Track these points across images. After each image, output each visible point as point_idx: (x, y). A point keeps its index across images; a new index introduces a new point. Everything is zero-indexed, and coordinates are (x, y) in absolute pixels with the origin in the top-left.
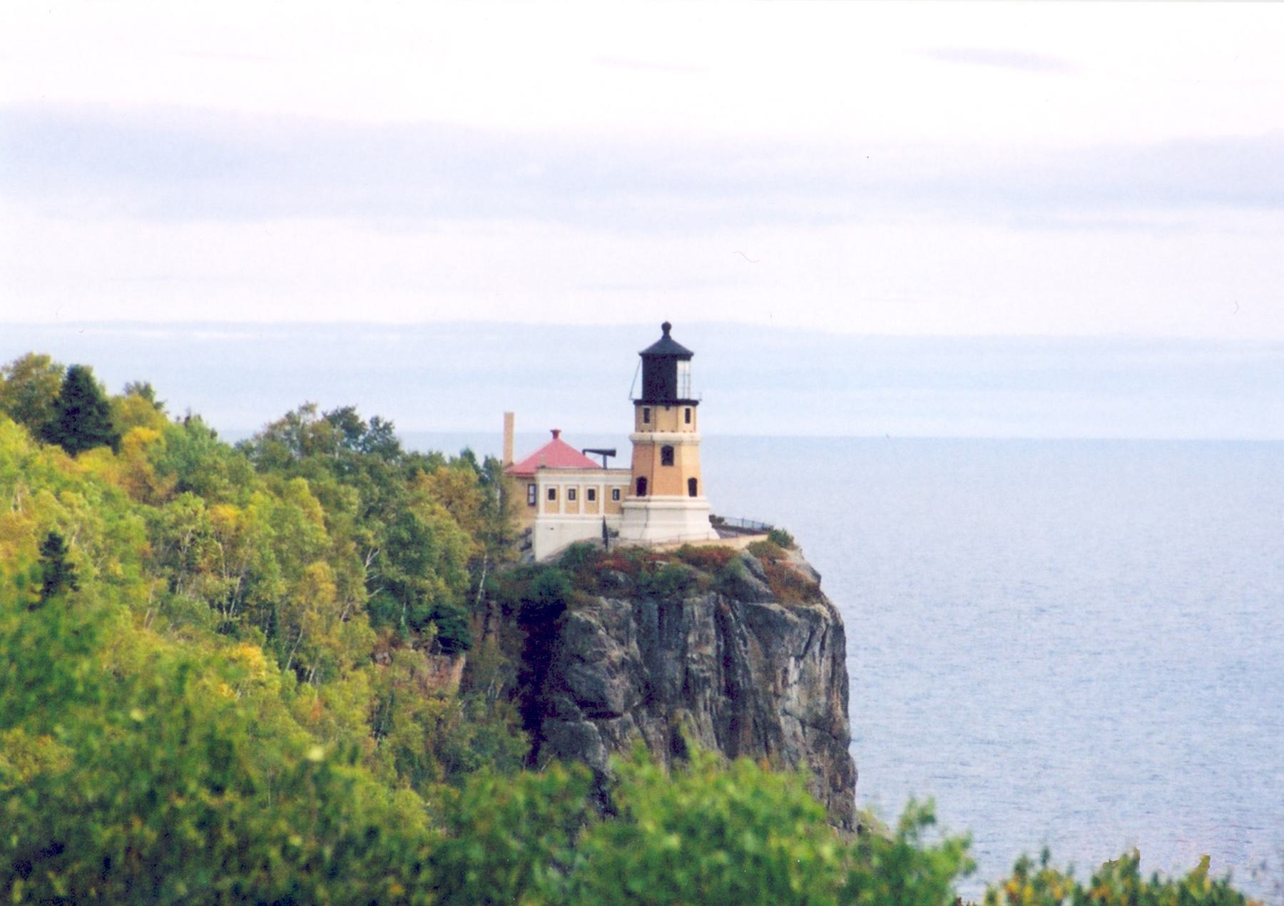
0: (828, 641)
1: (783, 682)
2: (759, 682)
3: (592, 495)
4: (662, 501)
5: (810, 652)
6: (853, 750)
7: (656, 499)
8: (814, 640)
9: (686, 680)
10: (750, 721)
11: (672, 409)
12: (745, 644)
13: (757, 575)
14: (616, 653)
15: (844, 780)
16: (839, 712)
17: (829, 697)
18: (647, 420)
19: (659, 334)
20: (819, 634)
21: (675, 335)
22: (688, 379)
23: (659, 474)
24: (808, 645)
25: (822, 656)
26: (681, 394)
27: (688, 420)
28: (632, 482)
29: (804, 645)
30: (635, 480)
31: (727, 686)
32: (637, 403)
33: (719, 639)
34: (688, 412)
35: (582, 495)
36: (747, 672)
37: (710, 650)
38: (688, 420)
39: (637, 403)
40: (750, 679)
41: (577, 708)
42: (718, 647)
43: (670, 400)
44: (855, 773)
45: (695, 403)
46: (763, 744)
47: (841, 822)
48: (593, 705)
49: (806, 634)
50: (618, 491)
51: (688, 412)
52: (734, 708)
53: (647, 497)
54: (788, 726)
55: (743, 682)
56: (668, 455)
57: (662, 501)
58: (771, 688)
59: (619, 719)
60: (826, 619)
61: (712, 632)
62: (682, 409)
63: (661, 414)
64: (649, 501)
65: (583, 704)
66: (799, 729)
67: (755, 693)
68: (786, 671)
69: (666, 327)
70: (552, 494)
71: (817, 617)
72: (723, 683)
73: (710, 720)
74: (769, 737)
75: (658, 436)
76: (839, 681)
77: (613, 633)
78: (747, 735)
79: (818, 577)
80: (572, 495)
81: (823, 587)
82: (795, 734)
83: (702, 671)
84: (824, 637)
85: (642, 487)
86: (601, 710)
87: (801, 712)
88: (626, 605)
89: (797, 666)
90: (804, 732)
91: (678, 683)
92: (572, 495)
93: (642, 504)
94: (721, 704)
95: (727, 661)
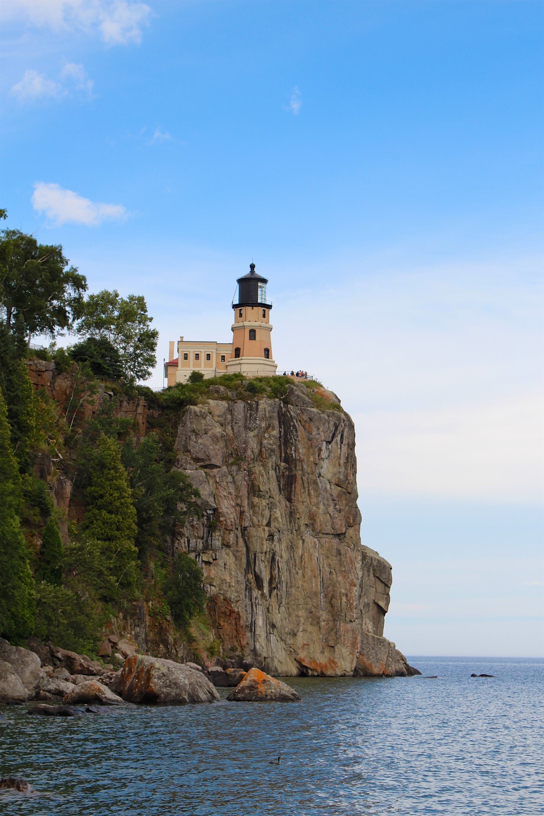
0: (345, 434)
1: (319, 456)
2: (304, 455)
3: (208, 357)
4: (248, 359)
5: (335, 440)
6: (359, 502)
7: (244, 359)
8: (338, 432)
9: (261, 449)
10: (300, 477)
11: (255, 308)
12: (296, 431)
13: (304, 394)
14: (218, 430)
15: (354, 521)
16: (351, 477)
17: (346, 468)
18: (241, 315)
20: (340, 429)
23: (248, 345)
24: (334, 436)
25: (342, 443)
26: (259, 301)
27: (264, 316)
28: (232, 351)
29: (331, 435)
30: (234, 350)
31: (285, 456)
32: (235, 306)
33: (280, 427)
34: (264, 310)
35: (203, 357)
37: (275, 433)
38: (264, 316)
39: (235, 306)
40: (299, 453)
41: (192, 462)
42: (280, 432)
43: (255, 304)
44: (361, 517)
45: (269, 307)
46: (307, 492)
47: (353, 545)
48: (203, 460)
49: (332, 428)
50: (223, 358)
51: (264, 310)
52: (289, 469)
53: (240, 358)
54: (323, 483)
55: (295, 455)
56: (253, 334)
57: (248, 359)
58: (312, 459)
59: (219, 469)
60: (344, 420)
61: (276, 423)
62: (261, 309)
63: (248, 311)
64: (242, 360)
65: (197, 460)
66: (328, 487)
67: (301, 461)
68: (320, 450)
69: (252, 267)
71: (339, 419)
72: (283, 455)
73: (275, 476)
74: (310, 489)
75: (246, 323)
77: (216, 418)
79: (340, 401)
80: (197, 356)
81: (342, 404)
82: (326, 488)
83: (270, 444)
84: (343, 431)
85: (237, 353)
86: (207, 463)
87: (329, 476)
88: (224, 404)
89: (327, 449)
90: (331, 488)
91: (256, 451)
92: (197, 356)
93: (238, 362)
94: (282, 468)
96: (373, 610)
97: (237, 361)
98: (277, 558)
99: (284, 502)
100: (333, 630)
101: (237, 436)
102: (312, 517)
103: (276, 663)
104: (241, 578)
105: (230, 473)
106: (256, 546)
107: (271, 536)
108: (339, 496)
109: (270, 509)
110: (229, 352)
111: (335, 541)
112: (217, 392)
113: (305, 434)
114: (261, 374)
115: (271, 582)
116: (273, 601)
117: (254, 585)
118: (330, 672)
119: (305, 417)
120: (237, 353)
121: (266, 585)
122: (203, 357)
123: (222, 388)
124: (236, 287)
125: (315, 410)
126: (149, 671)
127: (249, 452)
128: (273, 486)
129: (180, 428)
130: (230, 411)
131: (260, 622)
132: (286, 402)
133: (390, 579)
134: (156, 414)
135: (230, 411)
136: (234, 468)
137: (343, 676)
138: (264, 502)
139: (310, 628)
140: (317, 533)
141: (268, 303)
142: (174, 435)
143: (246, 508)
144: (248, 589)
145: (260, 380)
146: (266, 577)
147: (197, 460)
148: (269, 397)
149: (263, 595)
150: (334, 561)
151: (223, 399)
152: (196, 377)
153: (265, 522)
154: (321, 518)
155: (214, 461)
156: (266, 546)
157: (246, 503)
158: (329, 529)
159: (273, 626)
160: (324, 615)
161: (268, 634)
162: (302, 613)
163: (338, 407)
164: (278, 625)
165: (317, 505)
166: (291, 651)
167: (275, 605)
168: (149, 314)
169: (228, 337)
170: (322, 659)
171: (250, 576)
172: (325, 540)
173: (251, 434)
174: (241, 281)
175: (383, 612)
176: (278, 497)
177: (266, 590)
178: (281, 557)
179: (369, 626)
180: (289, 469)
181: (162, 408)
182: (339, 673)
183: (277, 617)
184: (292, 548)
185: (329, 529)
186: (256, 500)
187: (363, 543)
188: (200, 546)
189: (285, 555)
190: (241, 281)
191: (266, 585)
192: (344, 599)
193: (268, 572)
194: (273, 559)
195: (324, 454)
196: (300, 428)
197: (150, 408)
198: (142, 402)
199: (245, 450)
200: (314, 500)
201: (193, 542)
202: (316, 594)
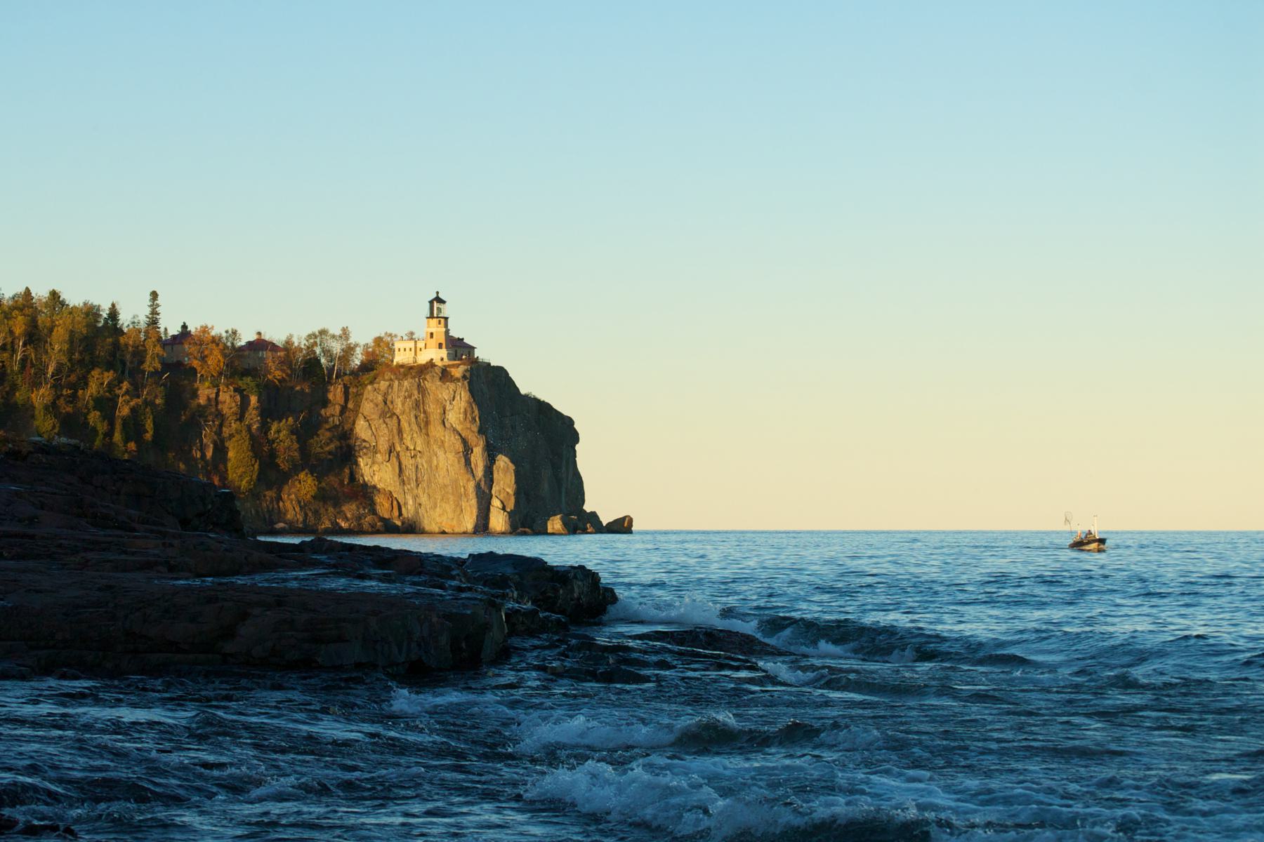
3: (411, 350)
19: (435, 296)
21: (440, 296)
35: (408, 350)
45: (446, 319)
61: (416, 392)
69: (438, 293)
78: (431, 428)
80: (405, 350)
88: (387, 383)
92: (405, 350)
98: (420, 467)
115: (416, 481)
118: (457, 530)
122: (408, 350)
124: (428, 304)
141: (445, 316)
144: (403, 483)
153: (412, 448)
157: (397, 437)
165: (444, 436)
177: (413, 484)
178: (423, 466)
180: (427, 418)
182: (462, 529)
184: (430, 462)
190: (431, 302)
192: (462, 489)
193: (414, 475)
194: (417, 467)
196: (431, 394)
202: (446, 486)
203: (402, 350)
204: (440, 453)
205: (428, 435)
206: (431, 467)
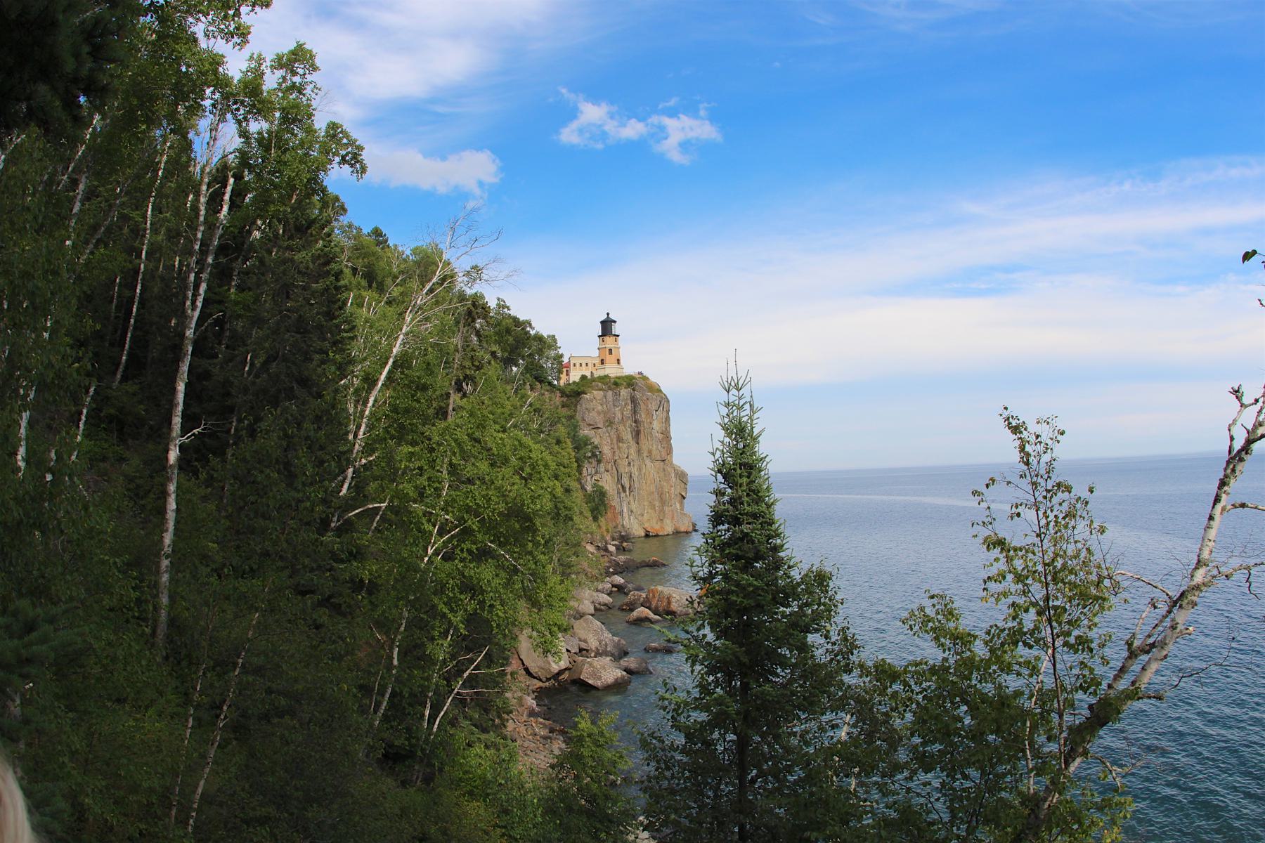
7: (607, 365)
22: (616, 329)
23: (608, 358)
32: (599, 336)
35: (584, 365)
36: (640, 416)
37: (629, 407)
45: (618, 336)
63: (607, 338)
67: (643, 422)
69: (608, 314)
70: (575, 365)
76: (668, 419)
78: (642, 436)
80: (581, 365)
85: (602, 362)
92: (581, 365)
95: (635, 412)
96: (679, 497)
97: (602, 366)
99: (635, 445)
100: (662, 511)
101: (609, 410)
102: (650, 452)
103: (634, 531)
104: (615, 487)
105: (607, 431)
106: (621, 470)
107: (629, 463)
108: (663, 439)
109: (628, 449)
110: (597, 361)
111: (662, 463)
112: (597, 386)
113: (645, 407)
114: (618, 375)
116: (631, 497)
117: (621, 490)
118: (660, 534)
119: (645, 398)
120: (602, 362)
121: (627, 490)
122: (584, 365)
123: (600, 384)
124: (599, 327)
125: (649, 394)
126: (668, 598)
127: (616, 419)
128: (630, 436)
129: (578, 407)
130: (605, 396)
131: (625, 510)
132: (634, 390)
133: (687, 480)
134: (565, 399)
135: (605, 396)
136: (609, 428)
137: (668, 535)
138: (625, 446)
139: (650, 511)
140: (652, 461)
142: (575, 411)
143: (616, 450)
144: (619, 493)
145: (619, 378)
146: (627, 486)
147: (590, 425)
148: (625, 388)
149: (626, 496)
150: (662, 474)
151: (600, 390)
152: (583, 377)
154: (654, 452)
155: (599, 426)
156: (627, 469)
158: (658, 458)
159: (632, 511)
160: (657, 504)
161: (630, 516)
162: (646, 503)
163: (660, 391)
164: (634, 511)
166: (641, 524)
167: (632, 501)
168: (558, 345)
169: (596, 353)
170: (657, 527)
171: (619, 486)
172: (657, 463)
173: (617, 409)
174: (602, 322)
175: (684, 498)
176: (632, 443)
177: (628, 493)
179: (678, 506)
181: (567, 396)
183: (634, 507)
184: (640, 469)
185: (658, 458)
186: (621, 444)
187: (674, 462)
188: (593, 472)
189: (637, 474)
190: (602, 322)
191: (627, 490)
195: (654, 417)
197: (562, 397)
198: (559, 395)
199: (614, 418)
200: (651, 443)
201: (589, 470)
202: (653, 493)
203: (578, 365)
204: (648, 461)
205: (638, 443)
206: (640, 474)
